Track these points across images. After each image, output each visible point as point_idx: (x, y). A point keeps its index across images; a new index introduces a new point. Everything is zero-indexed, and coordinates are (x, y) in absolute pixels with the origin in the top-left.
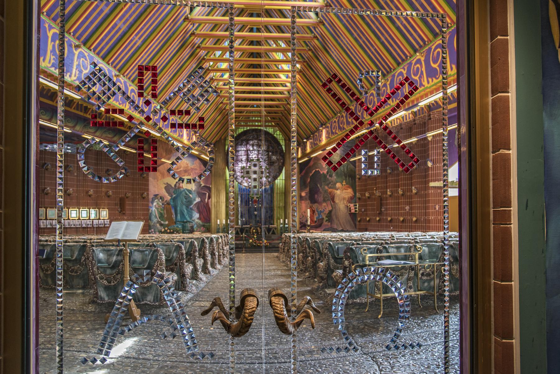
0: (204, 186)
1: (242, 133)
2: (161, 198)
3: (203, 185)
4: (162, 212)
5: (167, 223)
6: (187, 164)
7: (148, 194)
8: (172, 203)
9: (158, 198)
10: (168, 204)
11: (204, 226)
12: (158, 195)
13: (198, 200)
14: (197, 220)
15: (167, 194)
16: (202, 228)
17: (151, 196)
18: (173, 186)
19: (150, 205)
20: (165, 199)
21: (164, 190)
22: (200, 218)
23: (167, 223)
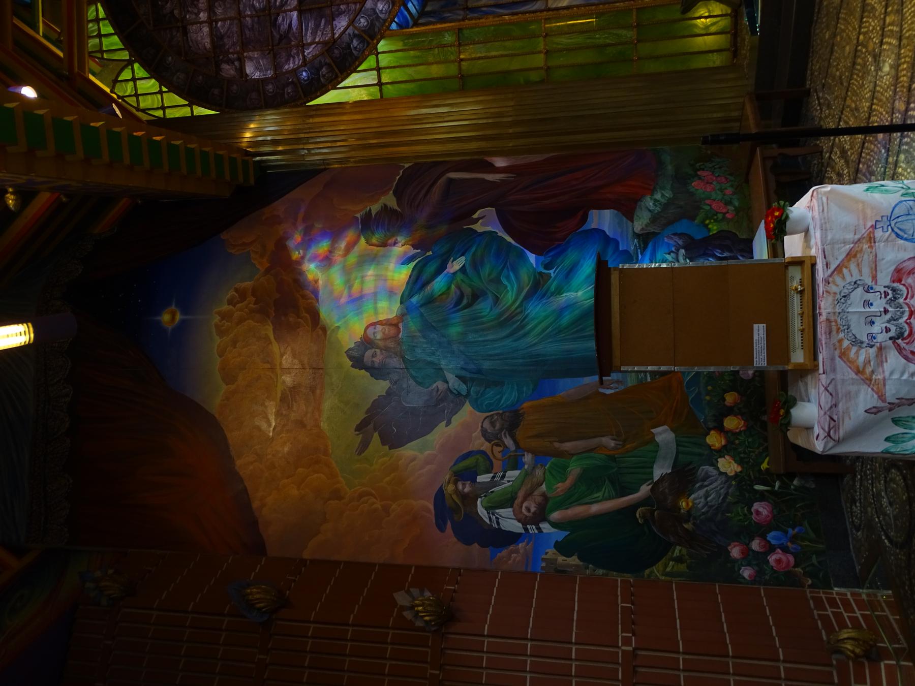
0: (398, 194)
1: (120, 30)
2: (469, 475)
3: (390, 200)
4: (575, 469)
5: (664, 435)
6: (242, 295)
7: (429, 576)
8: (509, 396)
9: (469, 500)
10: (513, 421)
11: (681, 180)
12: (440, 495)
13: (486, 222)
14: (640, 223)
15: (440, 433)
16: (696, 186)
17: (450, 551)
18: (381, 387)
19: (513, 557)
20: (479, 443)
21: (408, 451)
22: (627, 208)
23: (664, 435)
